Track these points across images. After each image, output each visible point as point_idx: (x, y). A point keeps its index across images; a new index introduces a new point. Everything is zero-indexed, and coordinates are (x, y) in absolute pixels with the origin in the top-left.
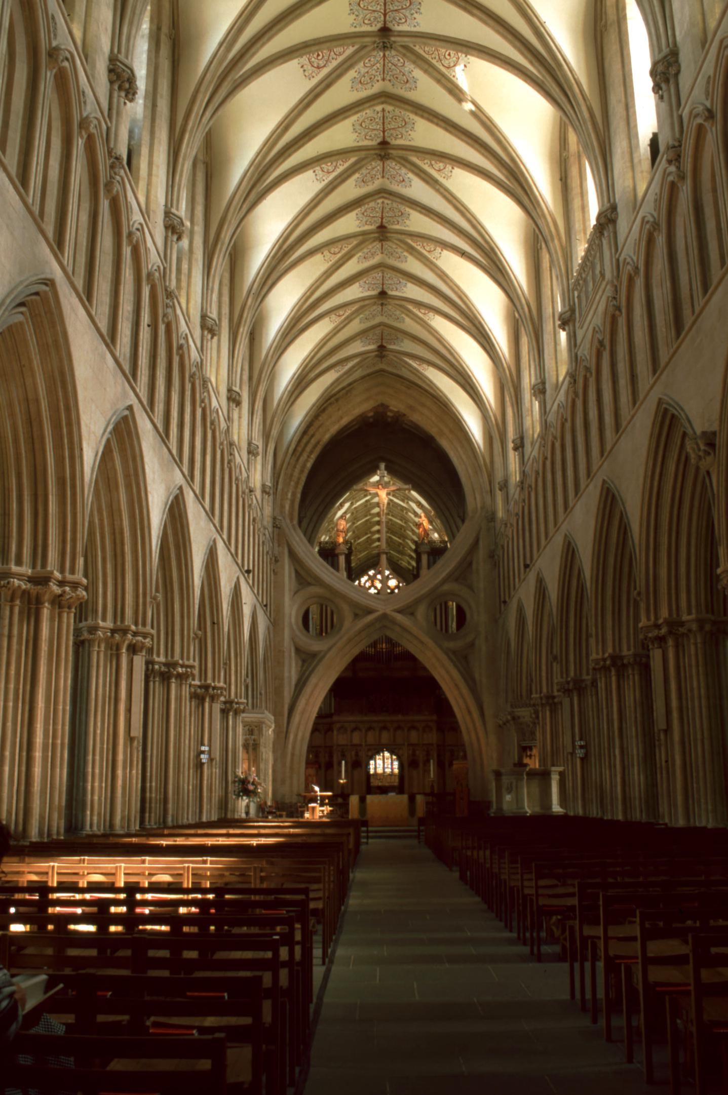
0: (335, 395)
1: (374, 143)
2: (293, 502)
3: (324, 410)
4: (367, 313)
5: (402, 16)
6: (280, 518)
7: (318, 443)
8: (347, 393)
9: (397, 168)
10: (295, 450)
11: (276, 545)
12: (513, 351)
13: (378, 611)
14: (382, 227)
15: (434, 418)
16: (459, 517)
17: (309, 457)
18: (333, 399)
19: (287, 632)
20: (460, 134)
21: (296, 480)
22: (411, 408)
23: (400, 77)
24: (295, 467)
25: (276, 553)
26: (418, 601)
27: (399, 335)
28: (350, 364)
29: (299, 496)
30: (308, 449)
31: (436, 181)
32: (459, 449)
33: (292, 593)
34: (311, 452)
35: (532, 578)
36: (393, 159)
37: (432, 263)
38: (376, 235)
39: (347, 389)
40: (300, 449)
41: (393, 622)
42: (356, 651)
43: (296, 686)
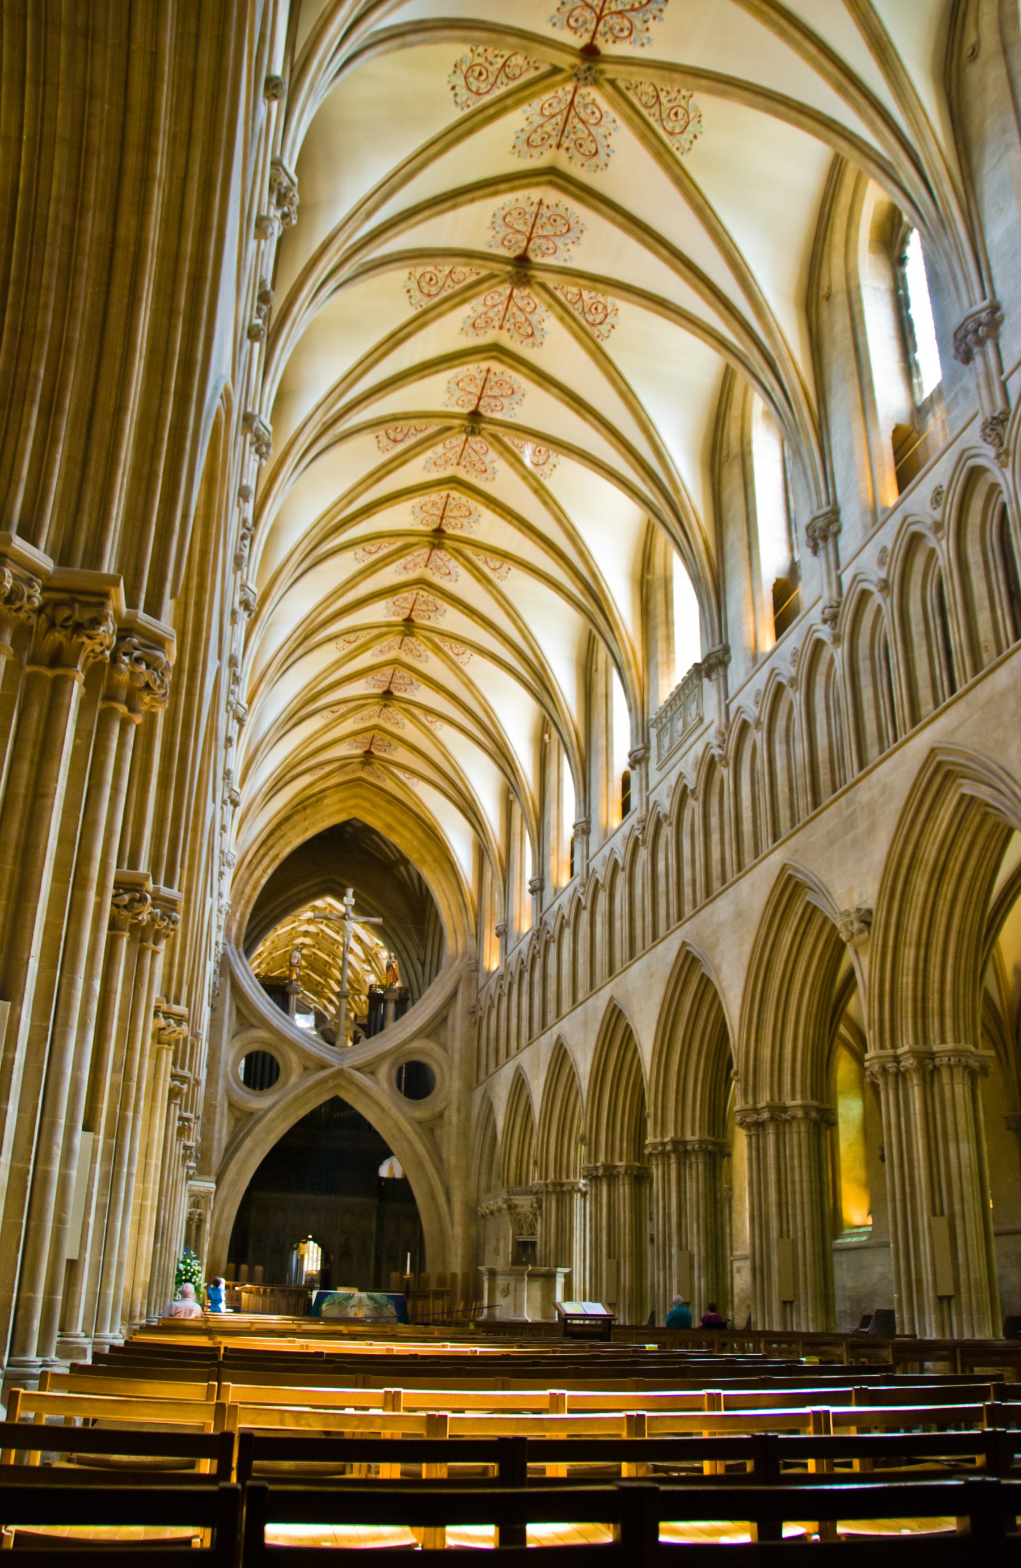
1: (428, 529)
4: (365, 712)
7: (277, 856)
8: (317, 801)
9: (446, 559)
10: (251, 862)
12: (538, 778)
13: (332, 1066)
14: (409, 620)
15: (415, 843)
16: (419, 959)
17: (264, 871)
18: (300, 807)
19: (221, 1085)
20: (535, 538)
22: (390, 827)
23: (478, 466)
24: (247, 882)
27: (395, 742)
28: (328, 769)
29: (248, 917)
30: (265, 862)
31: (489, 581)
32: (443, 881)
34: (268, 867)
35: (546, 1043)
36: (446, 550)
37: (458, 668)
38: (402, 628)
41: (352, 1082)
42: (302, 1112)
43: (226, 1150)
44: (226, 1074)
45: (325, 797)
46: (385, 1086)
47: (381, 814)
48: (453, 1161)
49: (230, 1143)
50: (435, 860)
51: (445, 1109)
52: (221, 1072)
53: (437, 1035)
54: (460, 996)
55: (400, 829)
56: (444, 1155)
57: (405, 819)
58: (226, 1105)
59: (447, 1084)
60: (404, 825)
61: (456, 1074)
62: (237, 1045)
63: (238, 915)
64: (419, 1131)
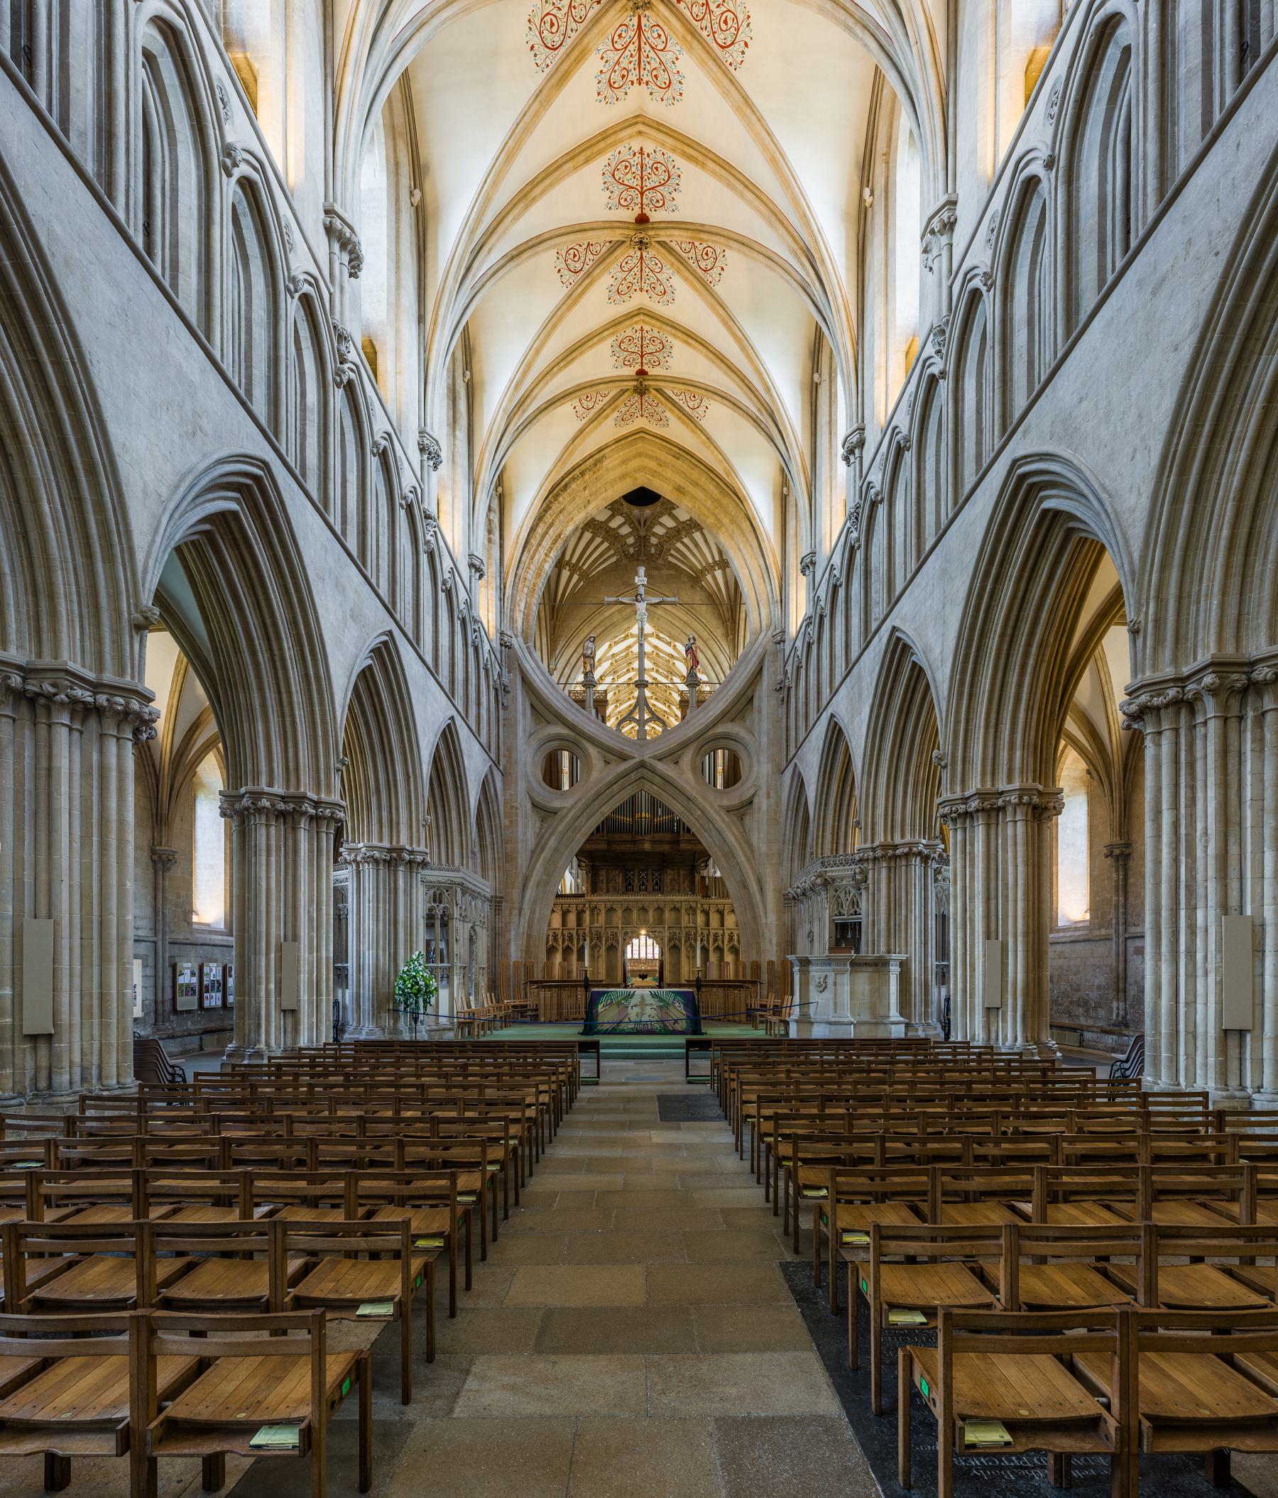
0: (578, 465)
3: (566, 486)
5: (659, 197)
6: (509, 633)
7: (559, 536)
8: (595, 465)
11: (505, 670)
15: (709, 503)
18: (577, 472)
22: (680, 489)
25: (505, 680)
26: (684, 745)
30: (547, 543)
39: (597, 457)
40: (534, 542)
45: (604, 456)
47: (669, 474)
48: (764, 848)
50: (733, 521)
51: (753, 796)
53: (743, 719)
54: (765, 672)
55: (690, 488)
56: (755, 842)
57: (695, 474)
59: (755, 769)
60: (695, 484)
61: (763, 758)
62: (534, 743)
64: (727, 819)
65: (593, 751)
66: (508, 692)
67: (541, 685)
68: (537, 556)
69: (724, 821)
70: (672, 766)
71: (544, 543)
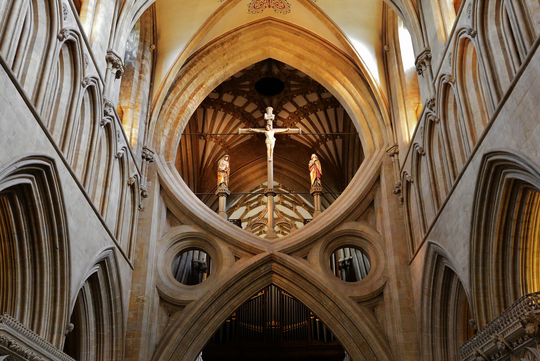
2: (169, 141)
3: (208, 52)
6: (151, 149)
7: (202, 85)
8: (233, 38)
11: (144, 178)
15: (324, 63)
17: (190, 98)
19: (150, 280)
21: (175, 119)
22: (300, 56)
24: (174, 105)
26: (312, 241)
30: (191, 89)
33: (161, 234)
40: (180, 87)
41: (283, 264)
44: (156, 270)
46: (320, 269)
47: (291, 46)
49: (162, 339)
52: (149, 267)
53: (366, 220)
58: (157, 299)
62: (167, 242)
63: (166, 132)
65: (224, 248)
66: (145, 196)
67: (177, 191)
68: (182, 97)
69: (357, 312)
70: (303, 260)
71: (188, 89)
